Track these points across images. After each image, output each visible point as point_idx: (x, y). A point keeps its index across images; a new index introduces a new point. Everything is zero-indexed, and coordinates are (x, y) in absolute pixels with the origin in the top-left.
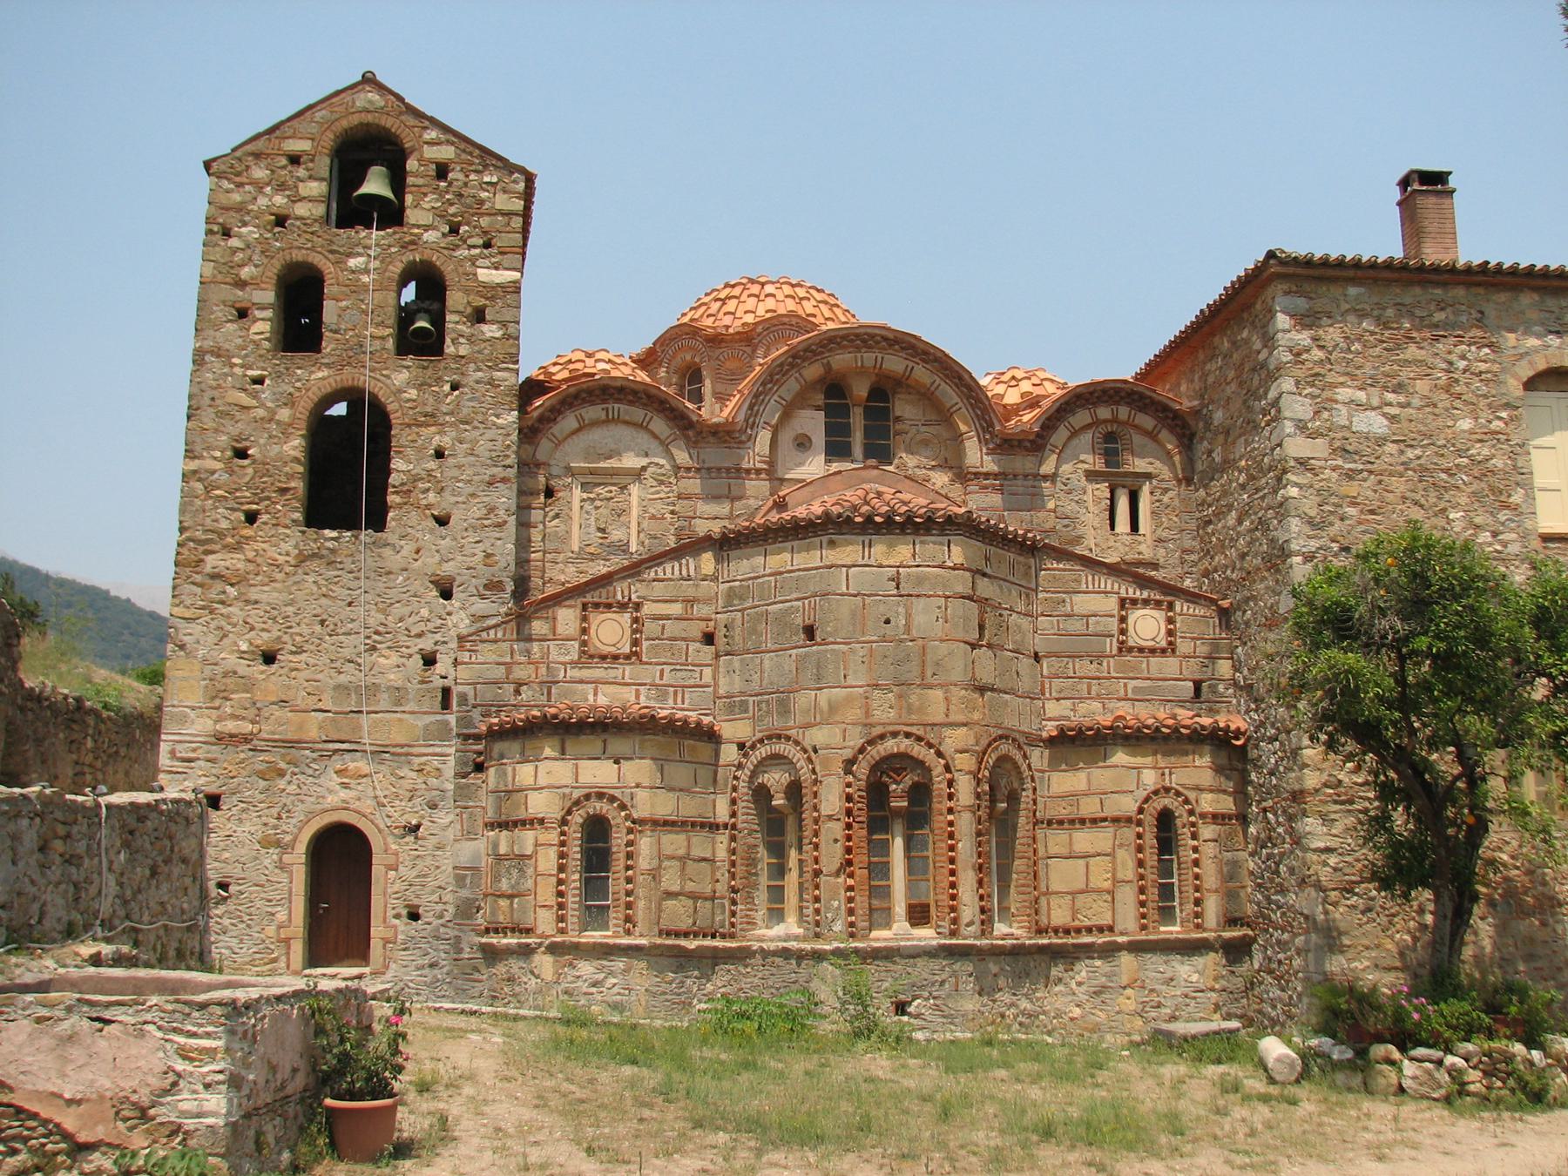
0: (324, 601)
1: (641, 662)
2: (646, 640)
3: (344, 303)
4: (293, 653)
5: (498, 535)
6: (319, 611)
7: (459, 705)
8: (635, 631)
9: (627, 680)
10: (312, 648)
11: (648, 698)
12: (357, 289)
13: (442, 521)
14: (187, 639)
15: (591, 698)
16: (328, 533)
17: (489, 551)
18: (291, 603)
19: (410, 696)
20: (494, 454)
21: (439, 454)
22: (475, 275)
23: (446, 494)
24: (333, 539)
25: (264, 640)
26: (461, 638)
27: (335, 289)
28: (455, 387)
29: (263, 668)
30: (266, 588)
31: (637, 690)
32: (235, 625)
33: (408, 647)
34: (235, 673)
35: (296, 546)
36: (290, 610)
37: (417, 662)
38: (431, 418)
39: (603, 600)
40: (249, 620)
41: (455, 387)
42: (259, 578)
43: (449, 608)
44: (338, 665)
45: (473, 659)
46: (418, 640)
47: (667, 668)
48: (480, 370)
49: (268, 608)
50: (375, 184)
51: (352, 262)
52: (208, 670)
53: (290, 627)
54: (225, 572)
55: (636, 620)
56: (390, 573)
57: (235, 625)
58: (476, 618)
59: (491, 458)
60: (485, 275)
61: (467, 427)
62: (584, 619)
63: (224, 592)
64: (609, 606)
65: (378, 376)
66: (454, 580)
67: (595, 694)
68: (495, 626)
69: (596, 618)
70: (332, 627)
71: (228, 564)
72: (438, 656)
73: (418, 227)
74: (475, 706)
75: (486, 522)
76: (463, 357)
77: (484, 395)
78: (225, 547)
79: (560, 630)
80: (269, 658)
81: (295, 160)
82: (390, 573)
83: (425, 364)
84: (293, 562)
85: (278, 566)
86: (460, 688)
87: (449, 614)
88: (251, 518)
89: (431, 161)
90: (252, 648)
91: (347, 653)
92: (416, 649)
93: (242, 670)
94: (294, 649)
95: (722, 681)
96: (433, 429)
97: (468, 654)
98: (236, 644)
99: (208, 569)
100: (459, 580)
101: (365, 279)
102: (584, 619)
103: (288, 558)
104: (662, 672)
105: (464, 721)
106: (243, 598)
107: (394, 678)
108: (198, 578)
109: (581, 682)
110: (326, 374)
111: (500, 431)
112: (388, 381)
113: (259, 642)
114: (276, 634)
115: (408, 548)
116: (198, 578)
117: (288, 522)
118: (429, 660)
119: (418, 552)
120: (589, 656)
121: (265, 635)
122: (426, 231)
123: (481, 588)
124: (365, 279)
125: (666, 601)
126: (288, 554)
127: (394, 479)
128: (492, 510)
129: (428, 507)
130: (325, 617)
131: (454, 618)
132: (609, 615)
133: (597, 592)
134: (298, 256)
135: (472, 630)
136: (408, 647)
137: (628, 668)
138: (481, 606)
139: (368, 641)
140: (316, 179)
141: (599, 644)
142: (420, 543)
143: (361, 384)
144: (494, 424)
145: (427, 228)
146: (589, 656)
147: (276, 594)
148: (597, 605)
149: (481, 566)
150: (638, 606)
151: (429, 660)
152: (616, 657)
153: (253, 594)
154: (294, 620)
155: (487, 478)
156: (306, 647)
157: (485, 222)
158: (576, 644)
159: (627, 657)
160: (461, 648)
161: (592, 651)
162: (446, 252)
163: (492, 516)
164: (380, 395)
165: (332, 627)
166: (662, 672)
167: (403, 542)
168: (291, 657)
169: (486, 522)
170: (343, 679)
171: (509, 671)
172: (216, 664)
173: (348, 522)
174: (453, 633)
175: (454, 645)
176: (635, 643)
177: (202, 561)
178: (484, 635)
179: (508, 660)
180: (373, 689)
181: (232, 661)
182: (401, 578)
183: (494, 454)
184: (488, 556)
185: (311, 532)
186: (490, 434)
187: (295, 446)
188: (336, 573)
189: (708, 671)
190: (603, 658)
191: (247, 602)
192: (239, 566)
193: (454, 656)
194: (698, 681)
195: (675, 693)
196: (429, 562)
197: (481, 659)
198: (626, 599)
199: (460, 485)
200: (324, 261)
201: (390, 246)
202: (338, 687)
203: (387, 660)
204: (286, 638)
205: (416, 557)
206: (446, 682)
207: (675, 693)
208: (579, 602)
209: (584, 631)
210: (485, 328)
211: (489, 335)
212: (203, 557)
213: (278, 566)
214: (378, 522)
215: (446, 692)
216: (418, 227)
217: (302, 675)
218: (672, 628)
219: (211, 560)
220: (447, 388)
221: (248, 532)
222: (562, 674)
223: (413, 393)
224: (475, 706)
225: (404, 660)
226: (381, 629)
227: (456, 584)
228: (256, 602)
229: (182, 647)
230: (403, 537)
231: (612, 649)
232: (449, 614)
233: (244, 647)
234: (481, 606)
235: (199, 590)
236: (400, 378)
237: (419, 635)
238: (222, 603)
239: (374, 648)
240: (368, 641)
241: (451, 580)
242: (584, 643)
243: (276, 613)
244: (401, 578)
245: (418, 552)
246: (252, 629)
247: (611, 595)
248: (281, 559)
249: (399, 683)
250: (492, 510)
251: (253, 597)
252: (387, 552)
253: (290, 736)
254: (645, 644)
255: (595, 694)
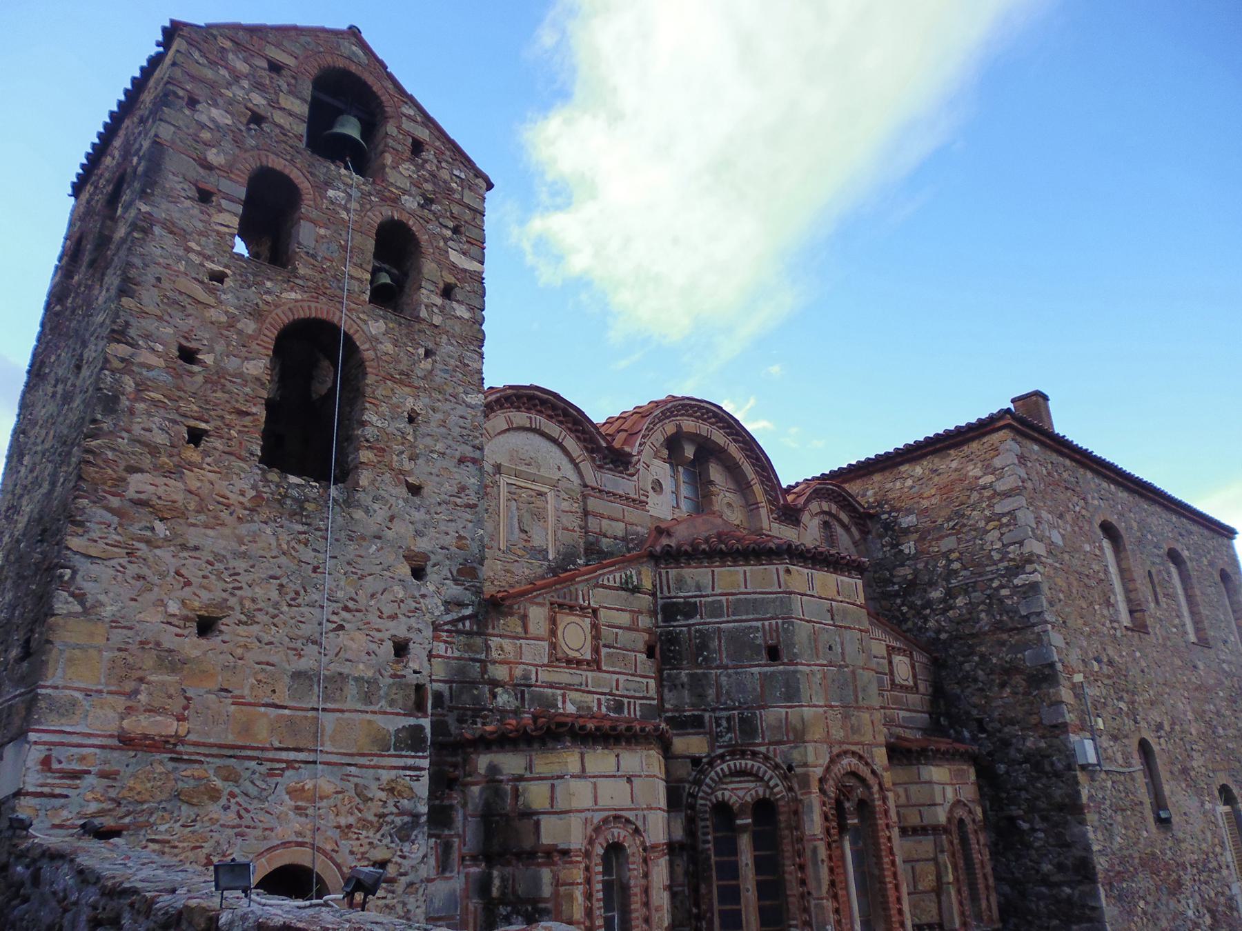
0: (283, 560)
1: (599, 669)
2: (605, 646)
3: (322, 231)
4: (240, 622)
5: (469, 517)
6: (279, 572)
7: (434, 707)
8: (593, 637)
9: (590, 689)
10: (266, 618)
11: (608, 708)
12: (331, 220)
13: (415, 490)
14: (88, 587)
15: (560, 705)
16: (293, 479)
17: (462, 533)
18: (244, 555)
19: (382, 692)
20: (465, 432)
21: (411, 420)
22: (447, 252)
23: (421, 461)
24: (298, 486)
25: (201, 600)
26: (436, 627)
27: (314, 214)
28: (428, 353)
29: (203, 641)
30: (210, 532)
31: (599, 700)
32: (162, 576)
33: (378, 630)
34: (158, 644)
35: (254, 487)
36: (241, 565)
37: (388, 647)
38: (405, 379)
39: (567, 601)
40: (183, 571)
41: (428, 353)
42: (202, 517)
43: (423, 591)
44: (299, 644)
45: (449, 650)
46: (391, 624)
47: (622, 678)
48: (452, 344)
49: (211, 559)
50: (351, 128)
51: (331, 193)
52: (118, 636)
53: (240, 588)
54: (155, 501)
55: (595, 627)
56: (363, 538)
57: (162, 576)
58: (449, 604)
59: (462, 436)
60: (454, 257)
61: (440, 397)
62: (553, 621)
63: (153, 529)
64: (571, 608)
65: (354, 317)
66: (428, 558)
67: (564, 702)
68: (469, 617)
69: (564, 619)
70: (293, 595)
71: (160, 491)
72: (411, 645)
73: (397, 188)
74: (451, 709)
75: (458, 501)
76: (436, 327)
77: (455, 371)
78: (156, 468)
79: (532, 629)
80: (206, 626)
81: (275, 67)
82: (363, 538)
83: (402, 321)
84: (248, 505)
85: (228, 506)
86: (436, 686)
87: (423, 596)
88: (196, 437)
89: (408, 134)
90: (185, 612)
91: (306, 630)
92: (387, 635)
93: (169, 640)
94: (244, 618)
95: (667, 695)
96: (407, 389)
97: (442, 646)
98: (161, 603)
99: (131, 493)
100: (434, 559)
101: (344, 215)
102: (553, 621)
103: (241, 499)
104: (617, 681)
105: (438, 727)
106: (179, 541)
107: (361, 670)
108: (115, 502)
109: (552, 687)
110: (299, 297)
111: (469, 410)
112: (365, 327)
113: (197, 604)
114: (219, 595)
115: (381, 514)
116: (115, 502)
117: (244, 453)
118: (401, 649)
119: (392, 519)
120: (558, 659)
121: (205, 595)
122: (404, 194)
123: (455, 573)
124: (344, 215)
125: (618, 610)
126: (242, 493)
127: (369, 431)
128: (463, 489)
129: (401, 472)
130: (284, 581)
131: (428, 601)
132: (573, 619)
133: (562, 593)
134: (277, 163)
135: (448, 618)
136: (378, 630)
137: (590, 674)
138: (454, 590)
139: (334, 618)
140: (298, 98)
141: (566, 649)
142: (395, 510)
143: (336, 321)
144: (464, 402)
145: (405, 192)
146: (558, 659)
147: (222, 543)
148: (561, 606)
149: (453, 549)
150: (595, 611)
151: (401, 649)
152: (579, 662)
153: (193, 536)
154: (244, 579)
155: (458, 455)
156: (260, 617)
157: (456, 209)
158: (545, 644)
159: (588, 663)
160: (436, 638)
161: (560, 655)
162: (421, 221)
163: (462, 495)
164: (355, 337)
165: (293, 595)
166: (617, 681)
167: (376, 506)
168: (241, 630)
169: (458, 501)
170: (304, 664)
171: (484, 670)
172: (131, 628)
173: (321, 475)
174: (428, 617)
175: (428, 633)
176: (596, 650)
177: (124, 480)
178: (460, 626)
179: (483, 656)
180: (340, 679)
181: (152, 619)
182: (374, 547)
183: (465, 432)
184: (460, 538)
185: (274, 476)
186: (461, 410)
187: (258, 366)
188: (301, 528)
189: (652, 683)
190: (569, 661)
191: (184, 547)
192: (175, 497)
193: (428, 647)
194: (645, 694)
195: (629, 703)
196: (401, 529)
197: (457, 654)
198: (586, 604)
199: (435, 456)
200: (303, 179)
201: (370, 194)
202: (297, 675)
203: (354, 642)
204: (232, 601)
205: (390, 525)
206: (423, 679)
207: (629, 703)
208: (548, 597)
209: (553, 633)
210: (455, 305)
211: (458, 313)
212: (124, 474)
213: (228, 506)
214: (346, 474)
215: (419, 688)
216: (397, 188)
217: (251, 657)
218: (624, 637)
219: (138, 484)
220: (422, 351)
221: (192, 454)
222: (534, 679)
223: (388, 347)
224: (451, 709)
225: (374, 646)
226: (351, 604)
227: (430, 563)
228: (196, 548)
229: (80, 598)
230: (376, 499)
231: (576, 654)
232: (423, 596)
233: (173, 608)
234: (454, 590)
235: (116, 519)
236: (377, 327)
237: (393, 617)
238: (148, 542)
239: (341, 627)
240: (334, 618)
241: (426, 558)
242: (553, 646)
243: (221, 566)
244: (374, 547)
245: (392, 519)
246: (188, 583)
247: (574, 597)
248: (234, 498)
249: (370, 674)
250: (463, 489)
251: (191, 544)
252: (359, 514)
253: (230, 739)
254: (604, 651)
255: (564, 702)
